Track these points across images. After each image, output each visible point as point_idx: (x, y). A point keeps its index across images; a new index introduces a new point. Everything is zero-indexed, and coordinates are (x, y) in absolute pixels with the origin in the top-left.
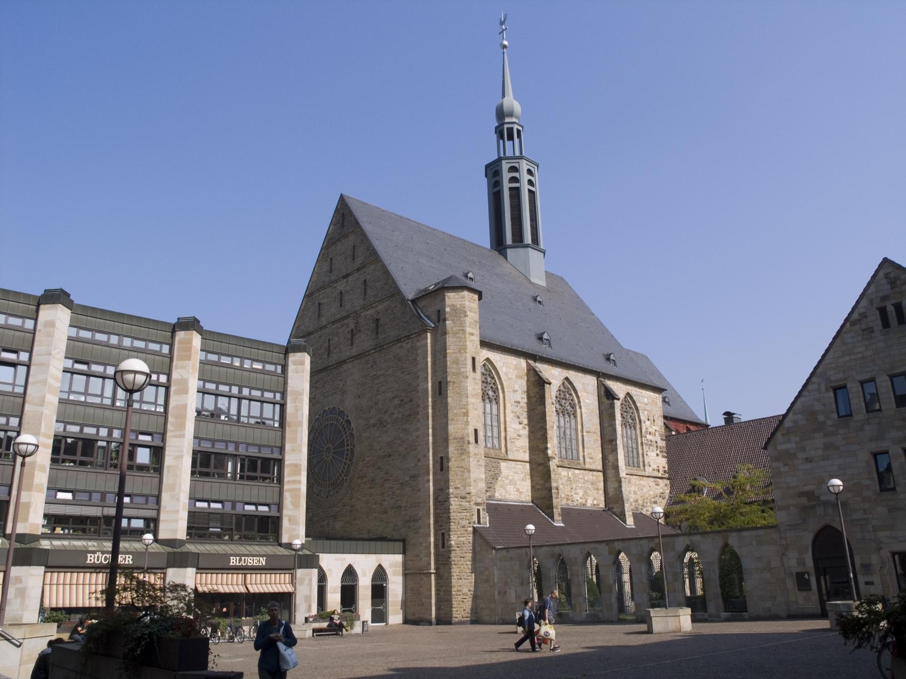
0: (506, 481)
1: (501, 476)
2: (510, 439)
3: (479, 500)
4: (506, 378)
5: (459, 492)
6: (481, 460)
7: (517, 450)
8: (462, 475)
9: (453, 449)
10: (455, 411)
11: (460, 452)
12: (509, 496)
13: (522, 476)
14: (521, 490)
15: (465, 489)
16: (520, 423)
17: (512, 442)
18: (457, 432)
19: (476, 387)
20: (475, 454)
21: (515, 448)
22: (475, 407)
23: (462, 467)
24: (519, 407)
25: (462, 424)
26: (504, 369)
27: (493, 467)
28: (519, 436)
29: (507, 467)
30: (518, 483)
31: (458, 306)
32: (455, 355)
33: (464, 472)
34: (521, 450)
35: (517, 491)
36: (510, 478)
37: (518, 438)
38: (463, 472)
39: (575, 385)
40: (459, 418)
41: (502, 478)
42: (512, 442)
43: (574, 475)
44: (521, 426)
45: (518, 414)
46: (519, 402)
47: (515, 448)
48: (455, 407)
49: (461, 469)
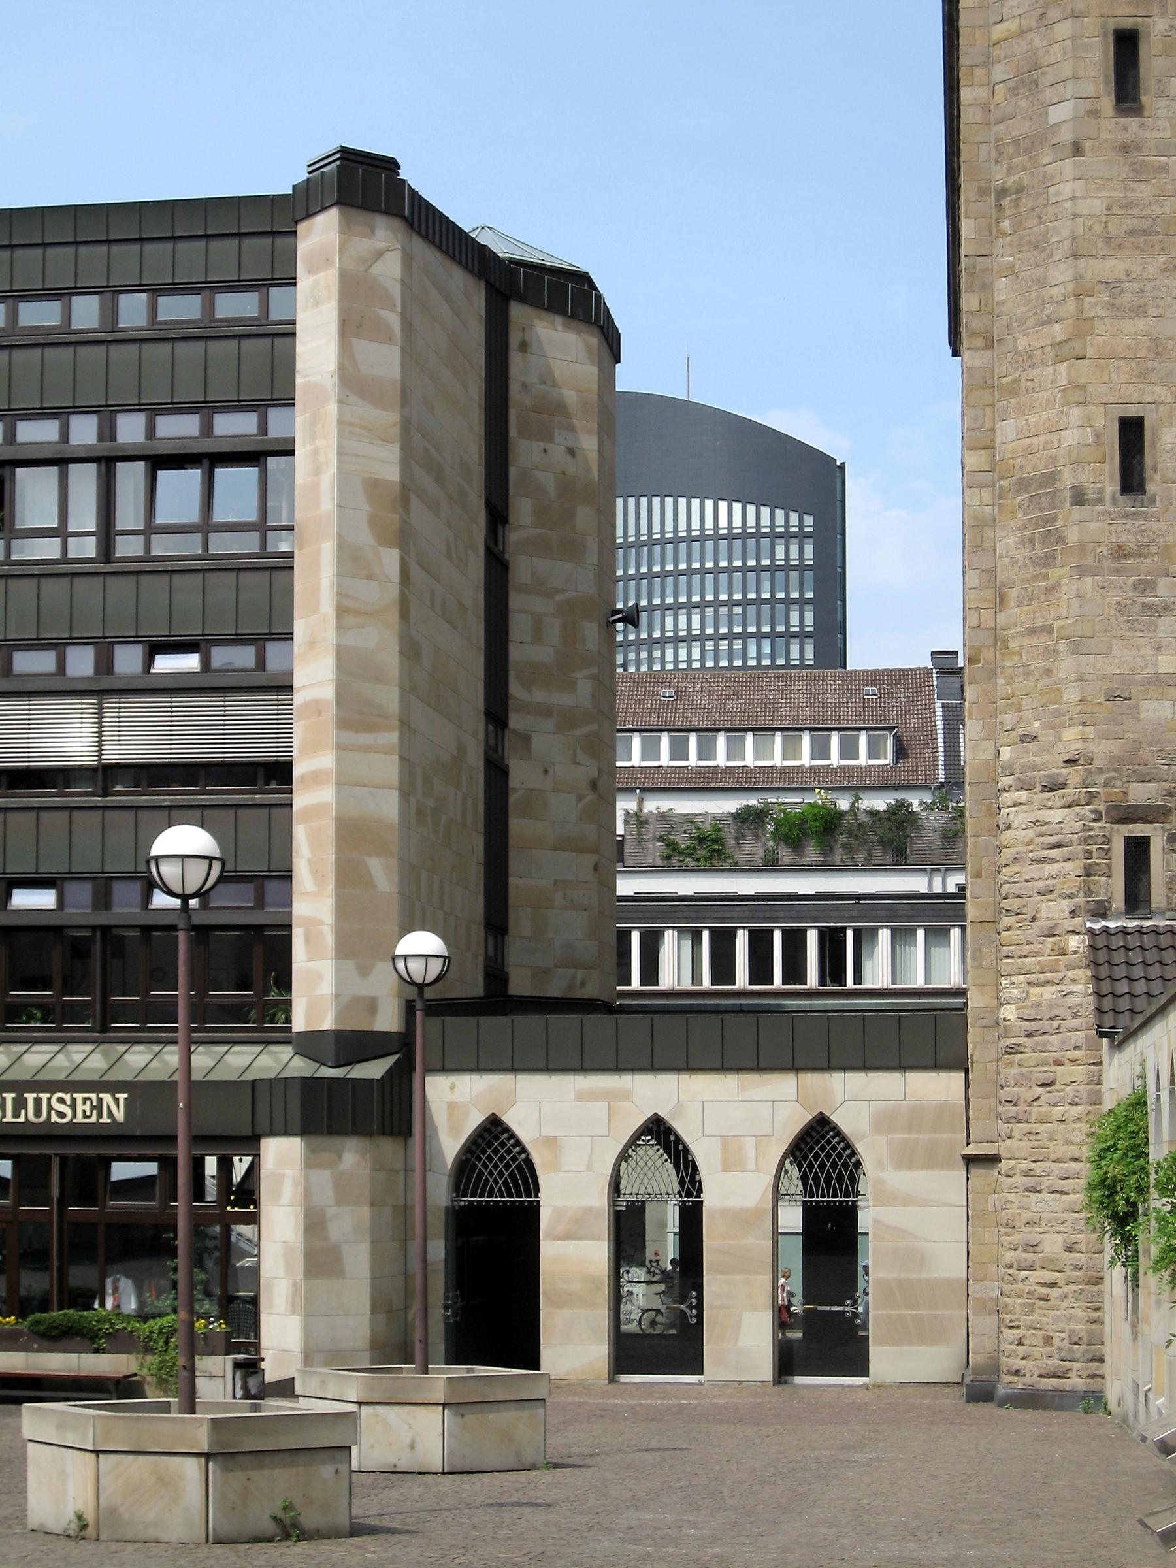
3: (1140, 793)
5: (1036, 759)
6: (1162, 582)
8: (1048, 672)
9: (1012, 540)
10: (1022, 343)
11: (1040, 550)
15: (1059, 739)
18: (1029, 451)
19: (1144, 191)
20: (1120, 553)
22: (1126, 299)
23: (1048, 630)
25: (1049, 404)
32: (1021, 45)
33: (1055, 651)
38: (1051, 653)
40: (1034, 373)
48: (1023, 321)
49: (1043, 640)
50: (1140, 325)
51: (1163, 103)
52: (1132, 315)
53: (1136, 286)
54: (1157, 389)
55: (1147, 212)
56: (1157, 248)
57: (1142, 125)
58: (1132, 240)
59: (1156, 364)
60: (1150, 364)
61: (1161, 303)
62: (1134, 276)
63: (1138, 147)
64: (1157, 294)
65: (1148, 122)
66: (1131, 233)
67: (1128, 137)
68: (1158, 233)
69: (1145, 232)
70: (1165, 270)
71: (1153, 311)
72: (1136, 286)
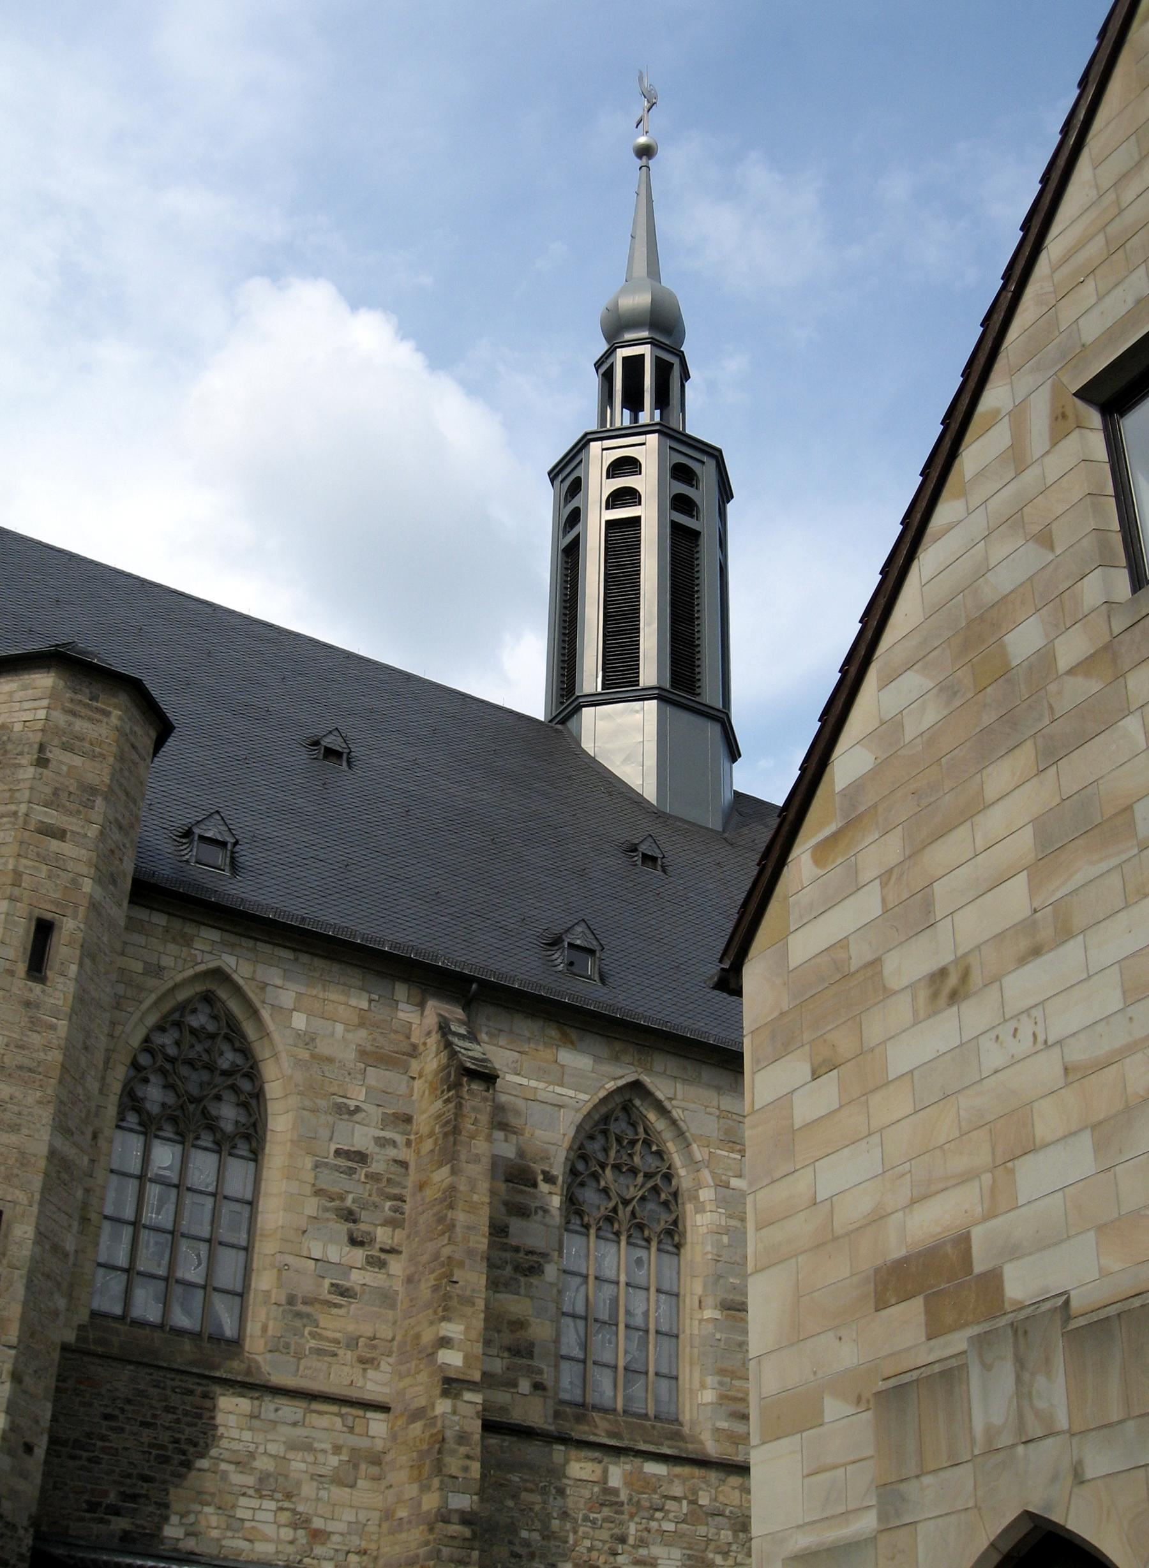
0: (238, 1478)
1: (214, 1452)
2: (291, 1300)
4: (305, 1055)
7: (319, 1352)
12: (245, 1545)
13: (334, 1461)
14: (318, 1523)
16: (354, 1242)
17: (298, 1315)
19: (36, 1039)
21: (313, 1343)
24: (361, 1175)
26: (299, 1021)
27: (169, 1409)
28: (344, 1292)
29: (253, 1417)
30: (308, 1489)
31: (18, 727)
34: (348, 1356)
35: (295, 1526)
36: (263, 1464)
37: (338, 1300)
39: (676, 1113)
41: (218, 1459)
42: (298, 1315)
43: (650, 1484)
44: (358, 1255)
45: (349, 1202)
46: (361, 1157)
47: (313, 1343)
50: (12, 1139)
51: (61, 979)
52: (9, 1130)
53: (16, 1108)
54: (17, 1192)
55: (35, 1055)
56: (37, 1083)
57: (43, 991)
58: (19, 1073)
59: (19, 1172)
60: (15, 1171)
61: (33, 1126)
62: (15, 1100)
63: (38, 1006)
64: (30, 1118)
65: (49, 990)
66: (20, 1068)
67: (32, 997)
68: (40, 1074)
69: (30, 1070)
70: (39, 1102)
71: (25, 1131)
72: (16, 1108)
